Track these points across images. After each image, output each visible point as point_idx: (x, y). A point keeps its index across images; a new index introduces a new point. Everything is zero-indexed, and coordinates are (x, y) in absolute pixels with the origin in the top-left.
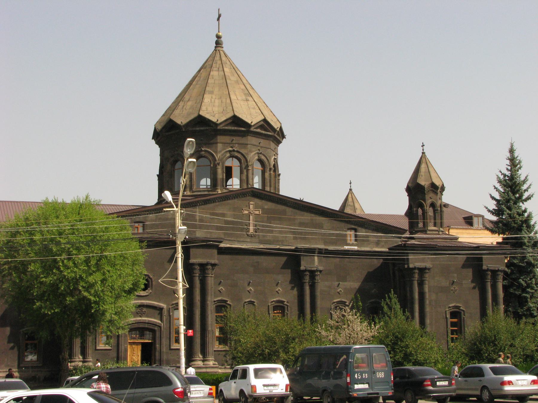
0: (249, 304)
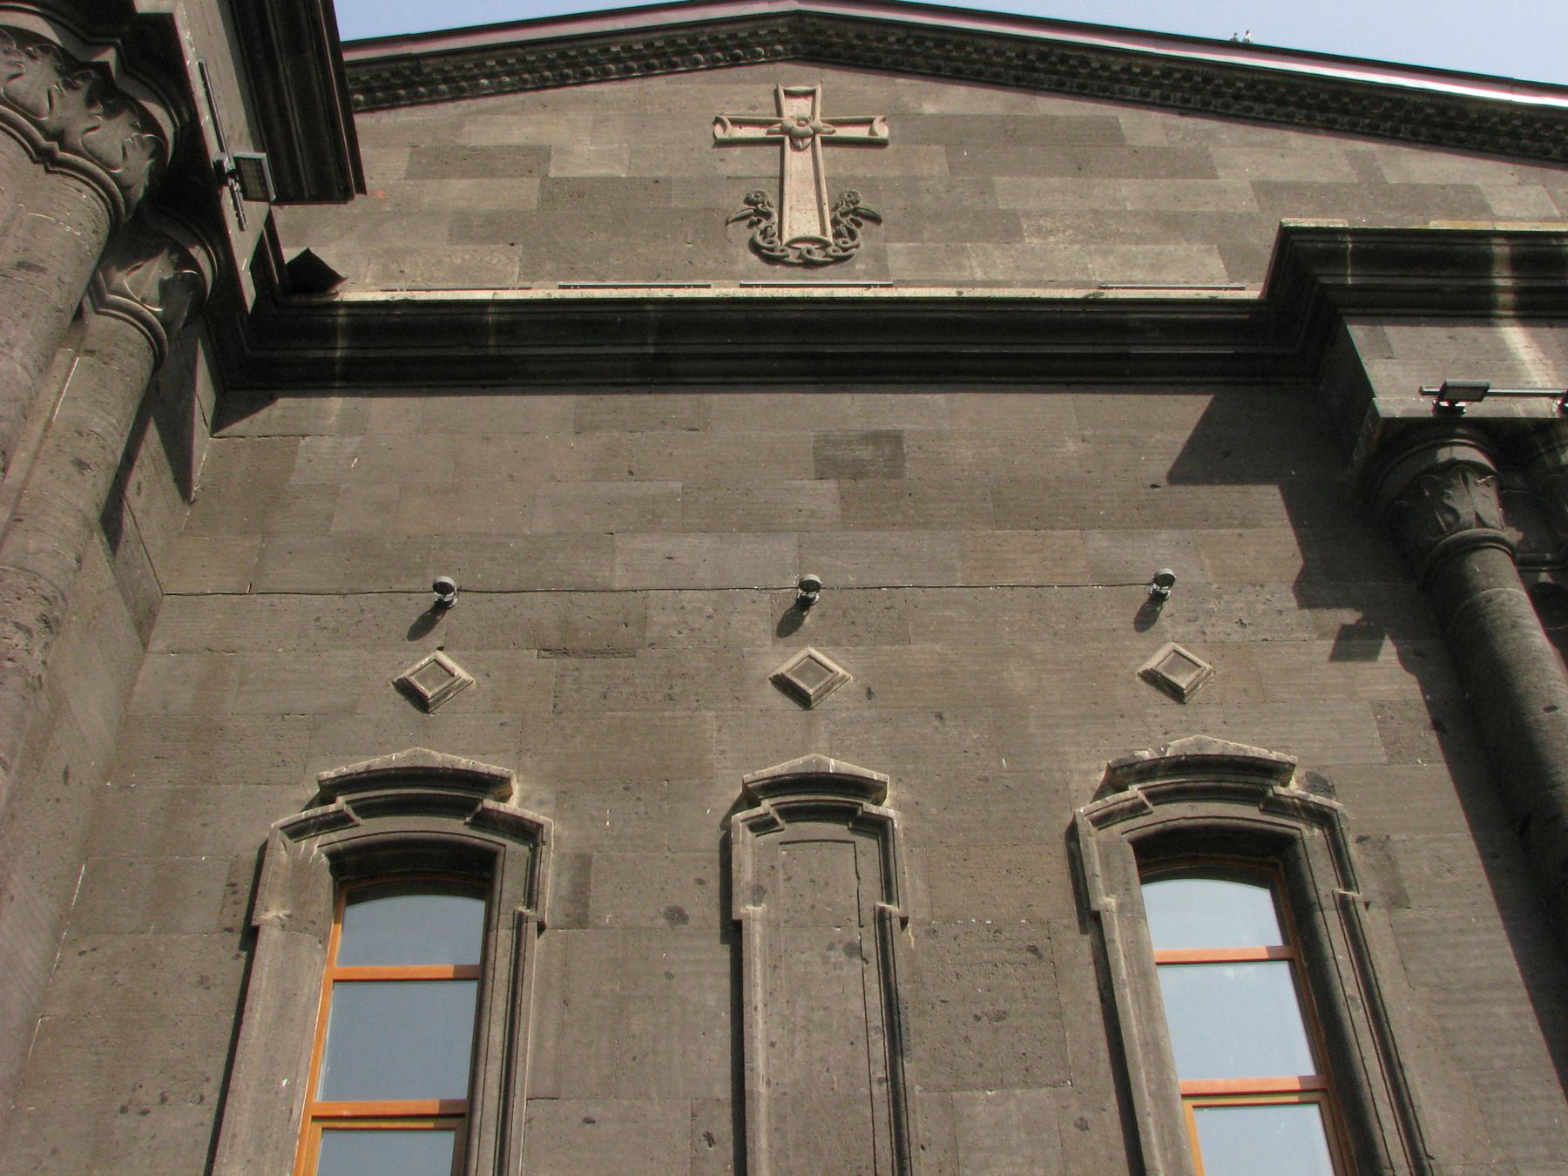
0: (791, 814)
